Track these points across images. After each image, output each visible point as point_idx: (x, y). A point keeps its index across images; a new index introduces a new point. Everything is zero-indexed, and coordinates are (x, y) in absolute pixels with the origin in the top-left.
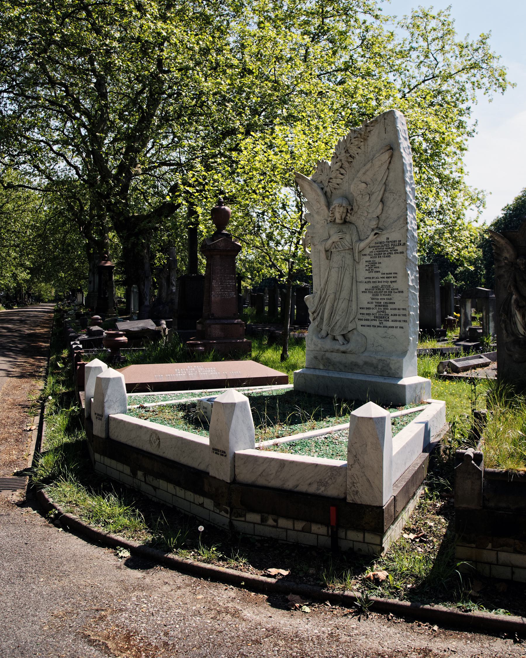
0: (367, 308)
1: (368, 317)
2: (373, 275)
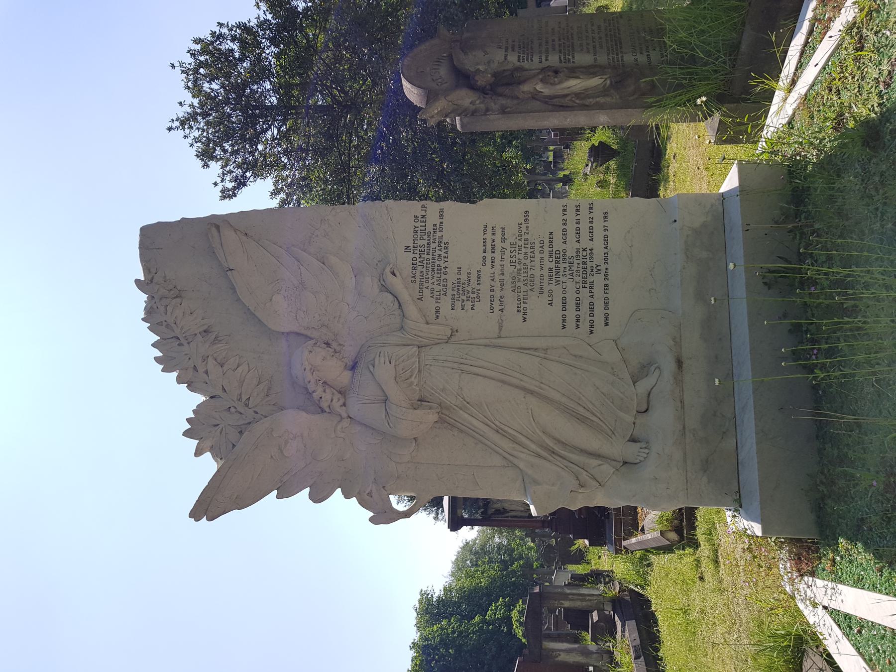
0: (564, 309)
1: (585, 307)
2: (485, 288)
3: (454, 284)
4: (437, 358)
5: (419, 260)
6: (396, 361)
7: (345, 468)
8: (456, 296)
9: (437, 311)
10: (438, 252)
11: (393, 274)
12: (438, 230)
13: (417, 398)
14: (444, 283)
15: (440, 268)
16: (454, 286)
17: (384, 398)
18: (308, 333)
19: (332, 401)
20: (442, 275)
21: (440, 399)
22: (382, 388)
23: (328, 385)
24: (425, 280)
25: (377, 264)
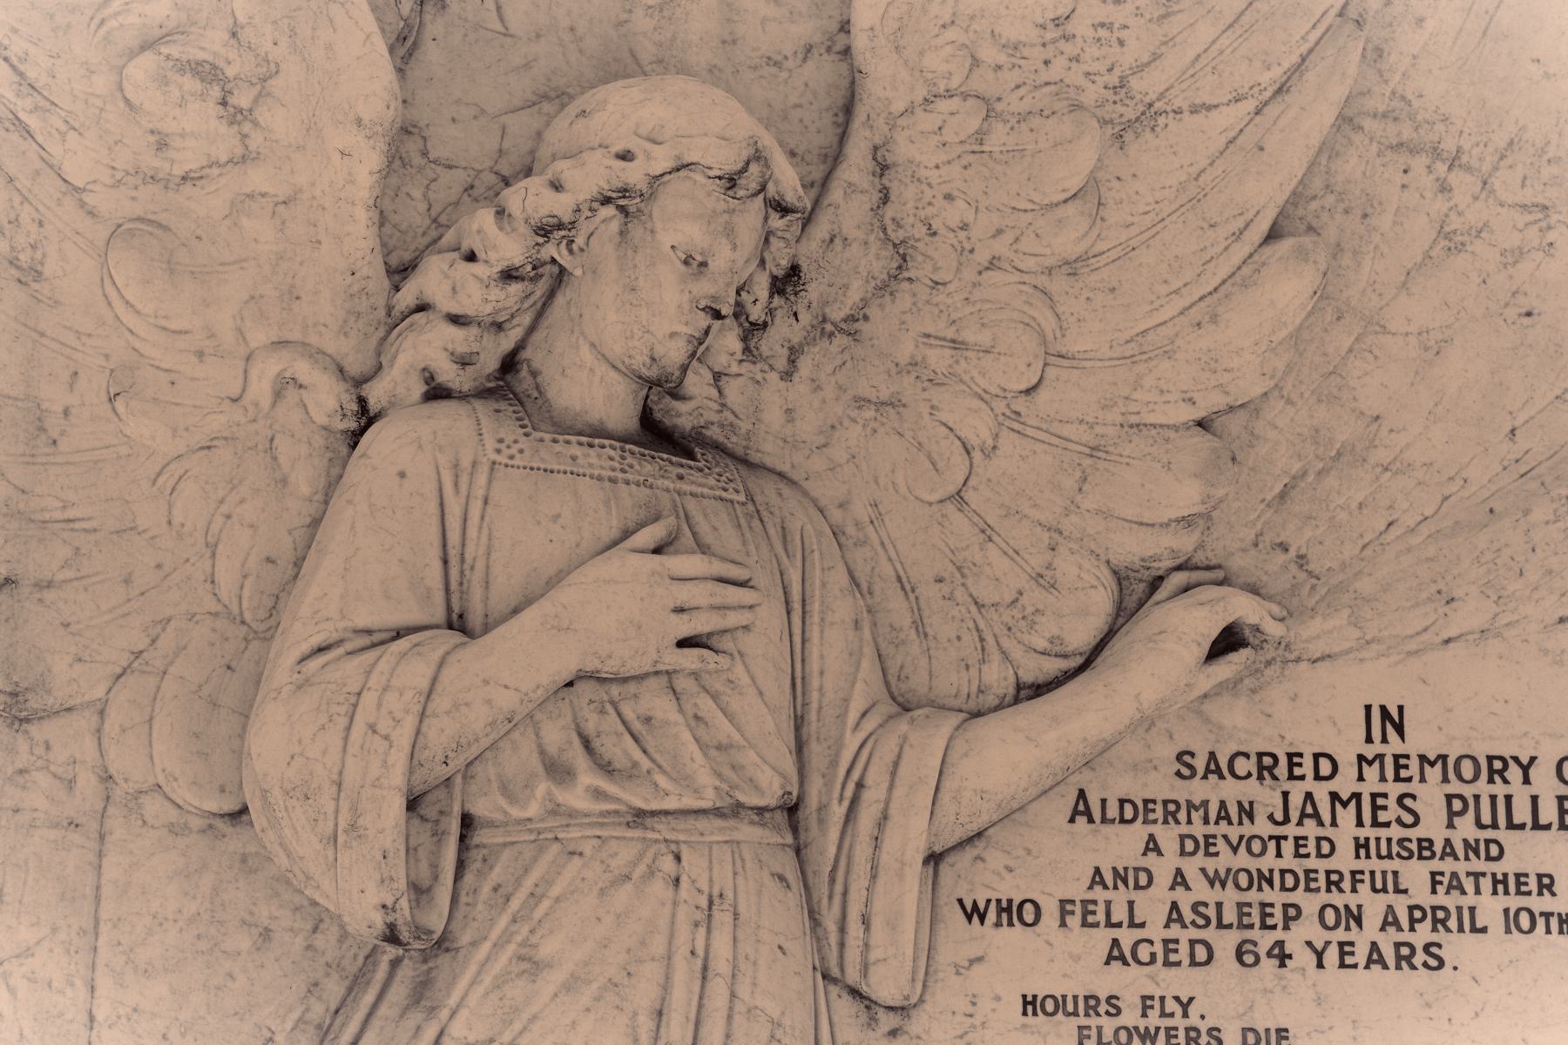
3: (1185, 1007)
4: (723, 918)
5: (1321, 792)
6: (695, 675)
7: (66, 412)
8: (1109, 1025)
9: (1011, 912)
10: (1374, 907)
11: (1228, 641)
12: (1514, 902)
13: (480, 809)
14: (1184, 948)
15: (1278, 918)
16: (1171, 1006)
17: (475, 619)
18: (856, 166)
19: (456, 320)
20: (1232, 938)
21: (474, 944)
22: (528, 601)
23: (551, 295)
24: (1198, 830)
25: (1284, 548)
